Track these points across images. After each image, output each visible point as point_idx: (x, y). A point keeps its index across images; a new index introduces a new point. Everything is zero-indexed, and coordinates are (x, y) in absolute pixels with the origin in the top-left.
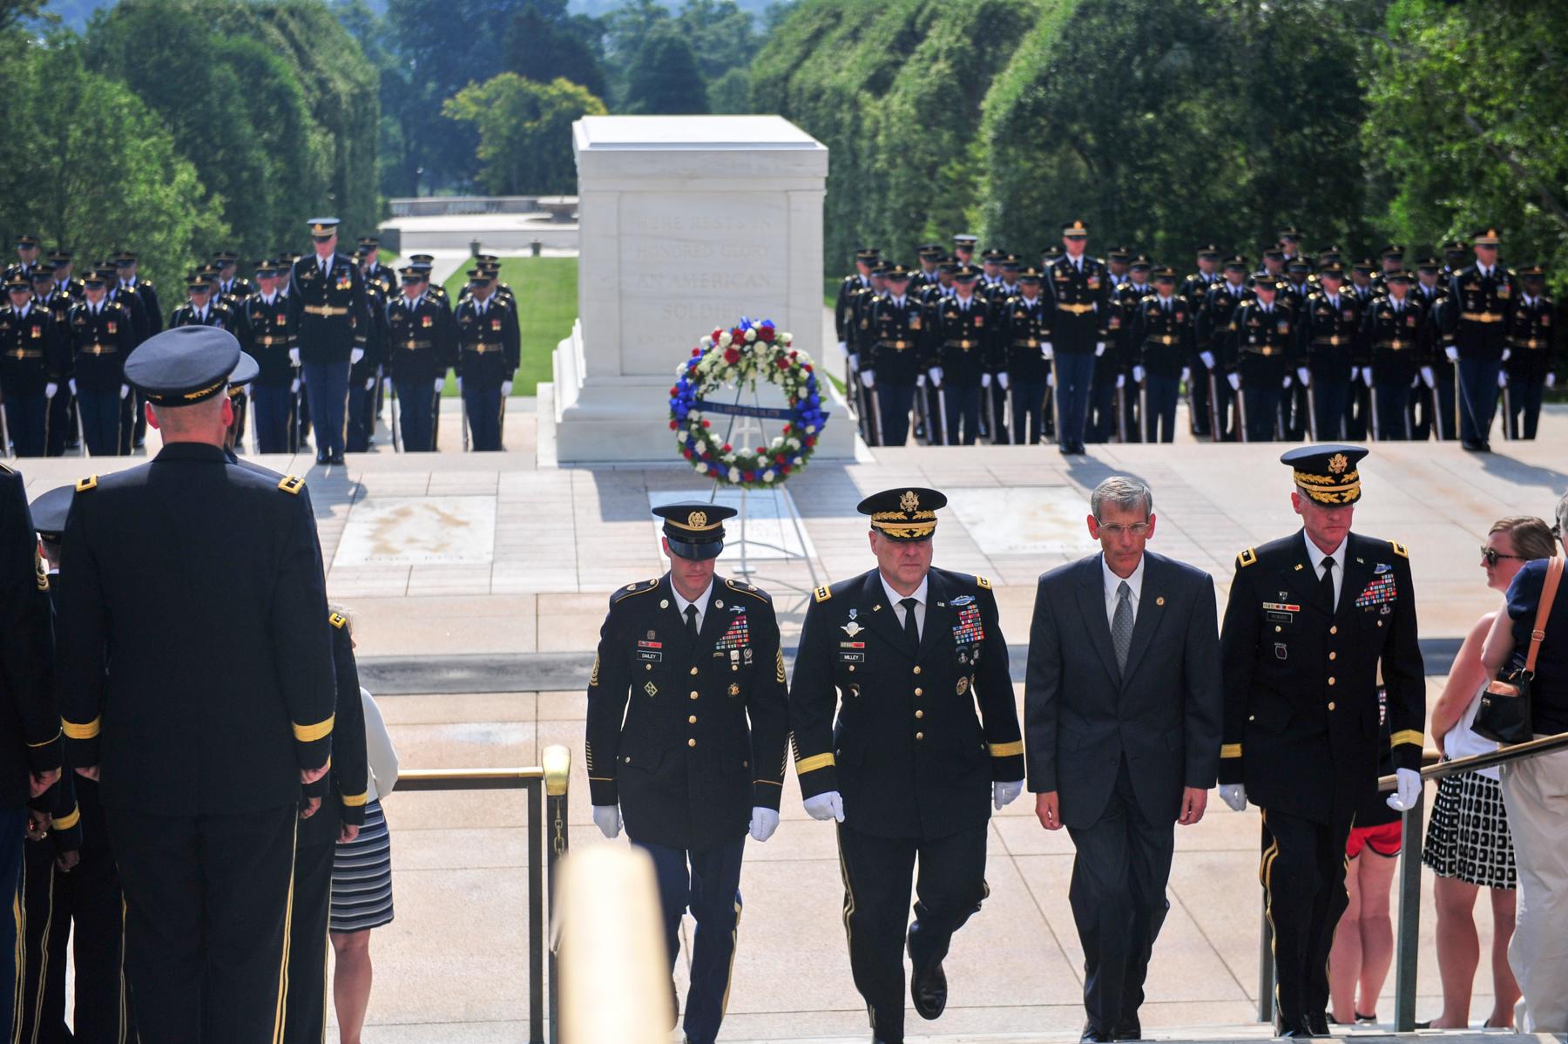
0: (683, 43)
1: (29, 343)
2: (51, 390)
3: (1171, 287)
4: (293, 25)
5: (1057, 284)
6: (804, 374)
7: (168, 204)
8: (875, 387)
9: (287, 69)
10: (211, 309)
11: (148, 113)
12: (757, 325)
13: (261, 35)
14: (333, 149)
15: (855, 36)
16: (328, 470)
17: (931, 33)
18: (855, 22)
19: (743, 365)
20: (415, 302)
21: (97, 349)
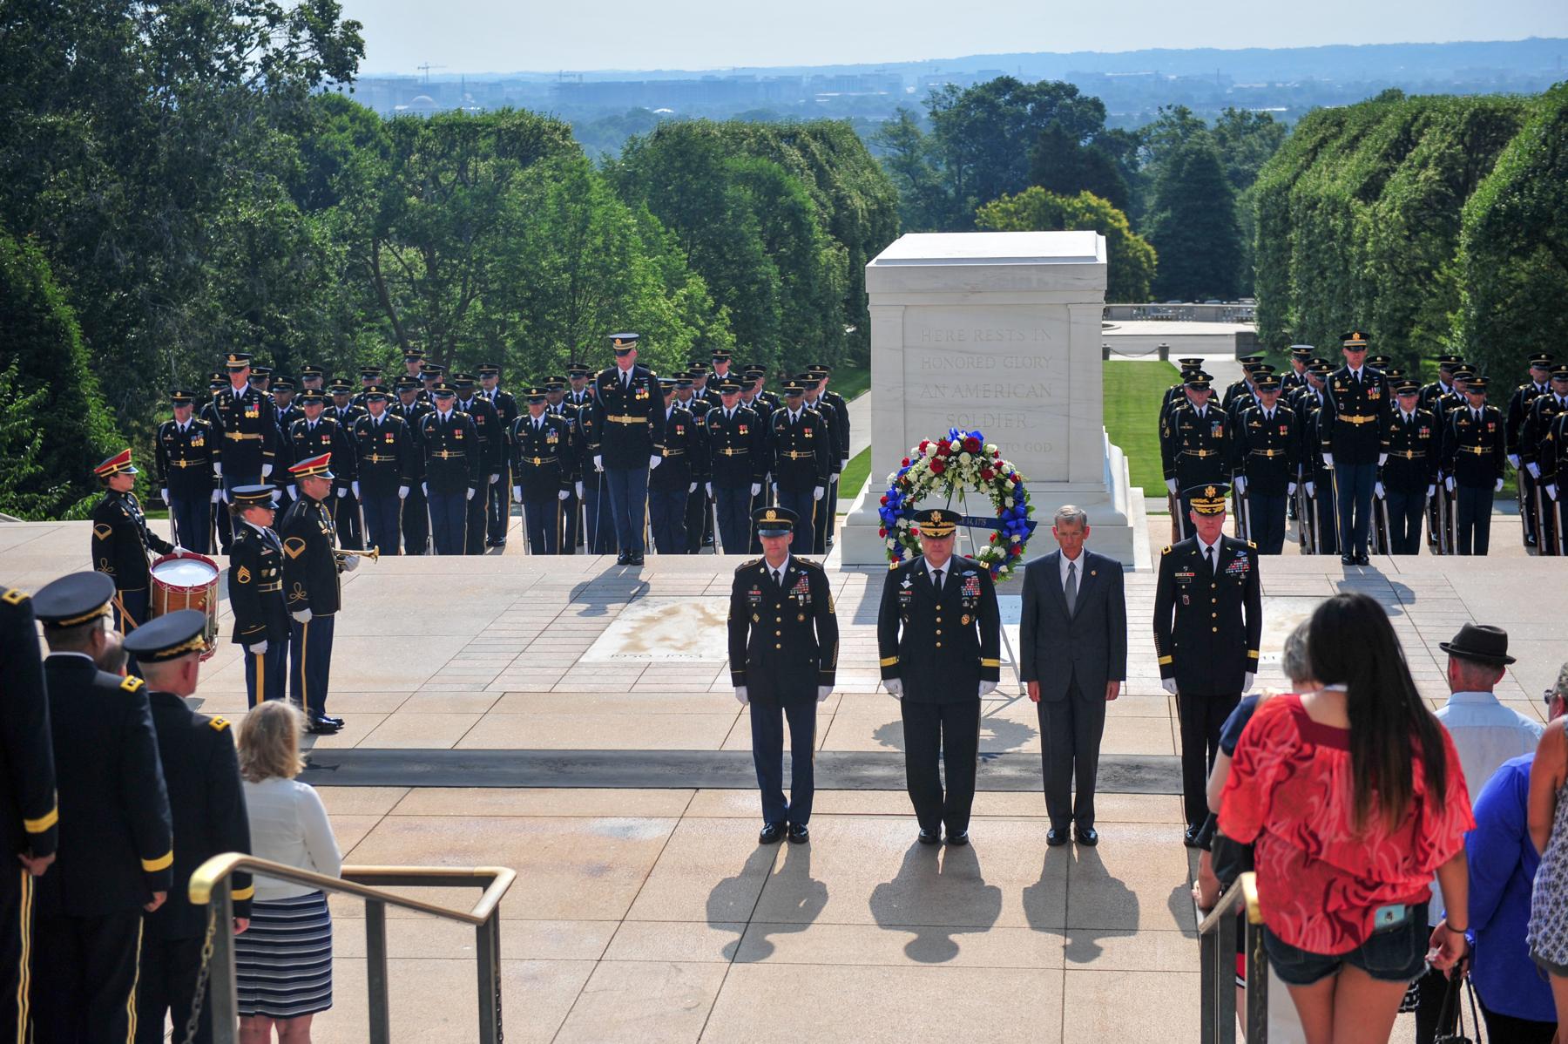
0: (1210, 154)
1: (383, 449)
2: (404, 491)
3: (1483, 397)
4: (815, 147)
5: (1336, 395)
6: (1010, 484)
7: (668, 317)
9: (803, 190)
12: (962, 436)
13: (780, 157)
15: (1353, 144)
17: (1422, 141)
18: (1355, 132)
19: (949, 475)
20: (733, 411)
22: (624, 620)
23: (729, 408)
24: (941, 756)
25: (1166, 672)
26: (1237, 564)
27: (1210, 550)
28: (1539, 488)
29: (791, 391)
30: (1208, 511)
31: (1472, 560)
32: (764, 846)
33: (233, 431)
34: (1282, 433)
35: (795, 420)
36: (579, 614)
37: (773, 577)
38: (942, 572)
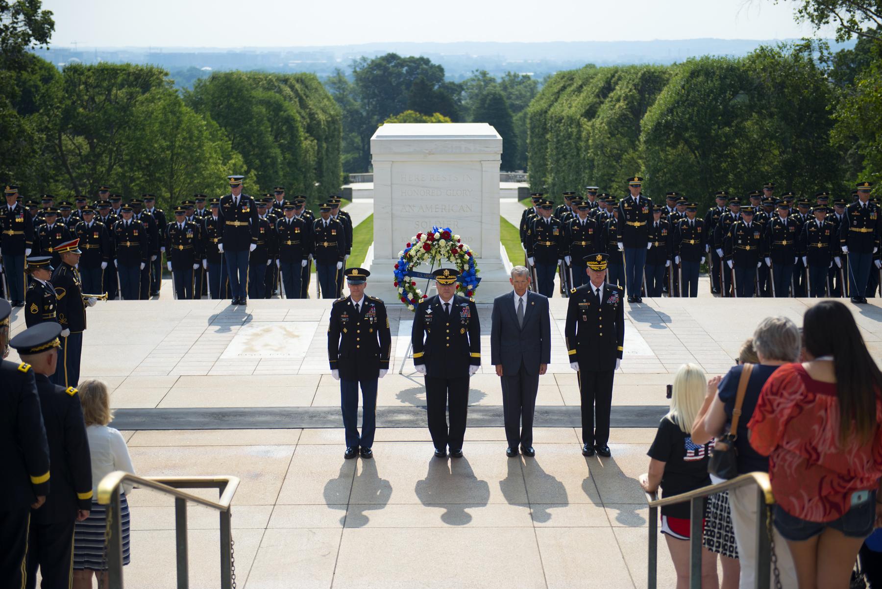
0: (500, 95)
2: (104, 265)
4: (298, 86)
5: (625, 211)
6: (467, 257)
8: (535, 266)
9: (292, 109)
10: (186, 224)
11: (221, 130)
12: (441, 230)
13: (280, 91)
14: (316, 148)
15: (580, 89)
16: (236, 308)
18: (580, 83)
19: (433, 252)
20: (291, 220)
21: (128, 244)
22: (241, 335)
23: (289, 218)
24: (447, 408)
25: (572, 359)
26: (613, 298)
27: (598, 290)
28: (722, 262)
29: (324, 209)
30: (598, 269)
31: (689, 299)
32: (348, 460)
33: (8, 230)
34: (590, 233)
35: (326, 225)
36: (215, 332)
37: (355, 307)
38: (449, 304)
